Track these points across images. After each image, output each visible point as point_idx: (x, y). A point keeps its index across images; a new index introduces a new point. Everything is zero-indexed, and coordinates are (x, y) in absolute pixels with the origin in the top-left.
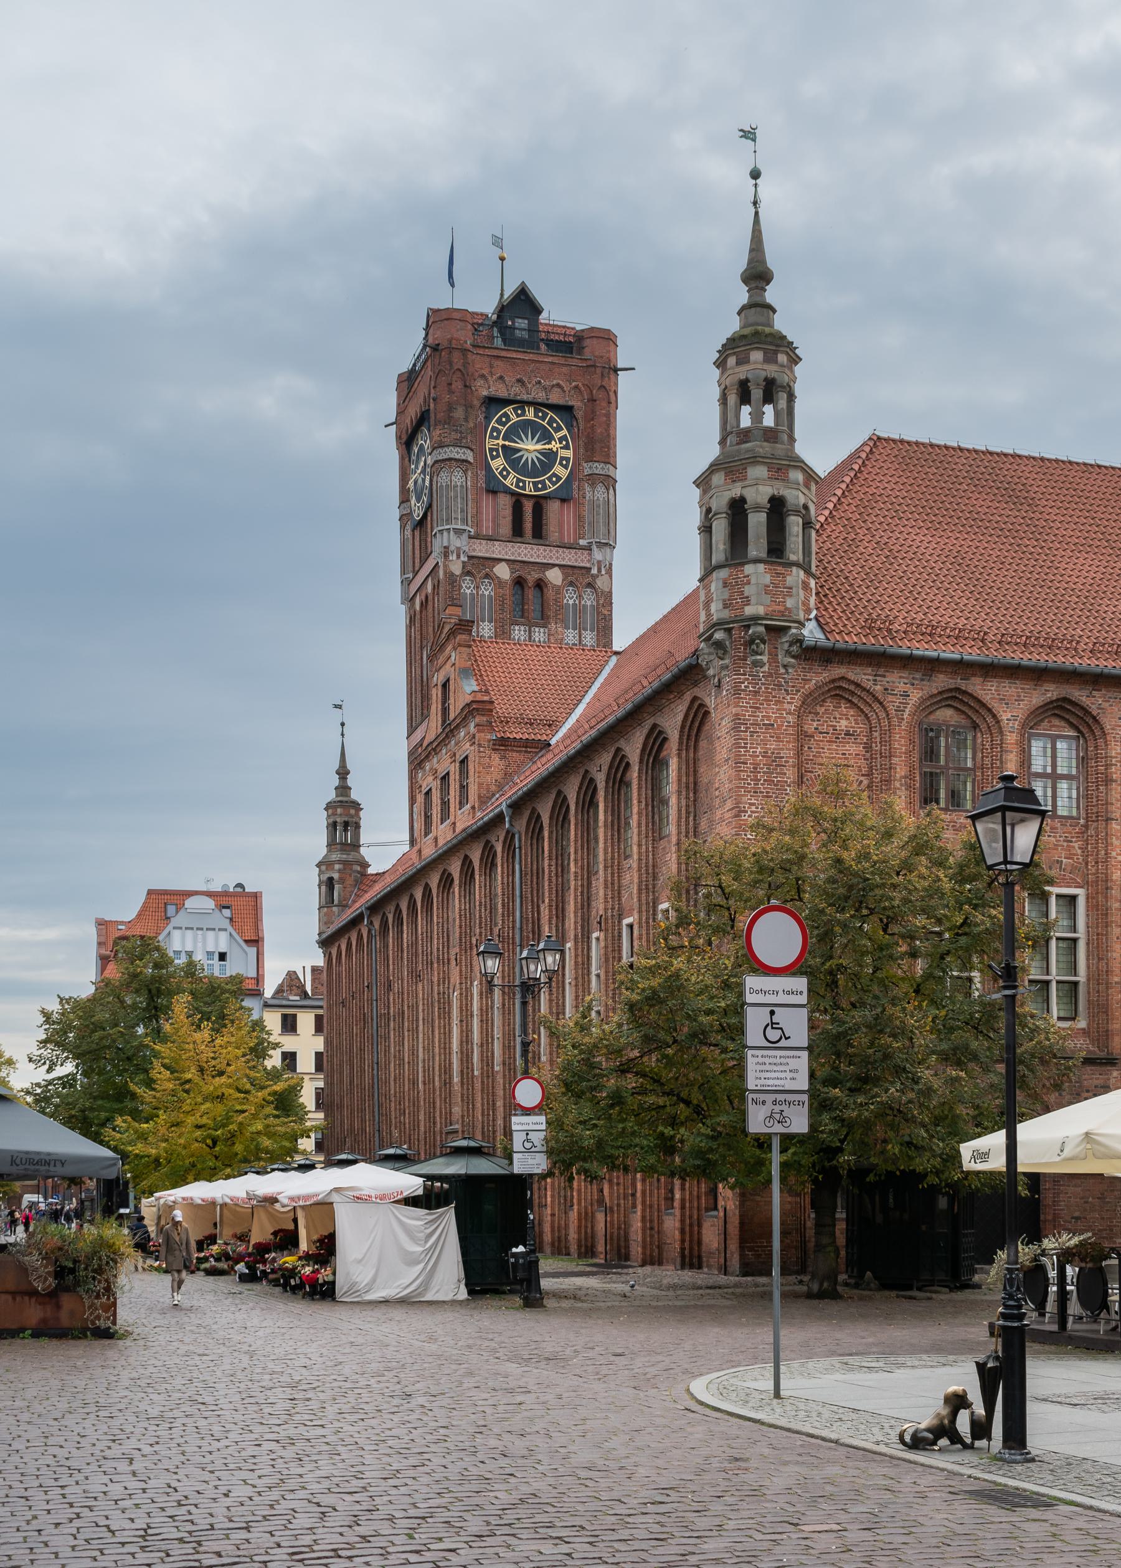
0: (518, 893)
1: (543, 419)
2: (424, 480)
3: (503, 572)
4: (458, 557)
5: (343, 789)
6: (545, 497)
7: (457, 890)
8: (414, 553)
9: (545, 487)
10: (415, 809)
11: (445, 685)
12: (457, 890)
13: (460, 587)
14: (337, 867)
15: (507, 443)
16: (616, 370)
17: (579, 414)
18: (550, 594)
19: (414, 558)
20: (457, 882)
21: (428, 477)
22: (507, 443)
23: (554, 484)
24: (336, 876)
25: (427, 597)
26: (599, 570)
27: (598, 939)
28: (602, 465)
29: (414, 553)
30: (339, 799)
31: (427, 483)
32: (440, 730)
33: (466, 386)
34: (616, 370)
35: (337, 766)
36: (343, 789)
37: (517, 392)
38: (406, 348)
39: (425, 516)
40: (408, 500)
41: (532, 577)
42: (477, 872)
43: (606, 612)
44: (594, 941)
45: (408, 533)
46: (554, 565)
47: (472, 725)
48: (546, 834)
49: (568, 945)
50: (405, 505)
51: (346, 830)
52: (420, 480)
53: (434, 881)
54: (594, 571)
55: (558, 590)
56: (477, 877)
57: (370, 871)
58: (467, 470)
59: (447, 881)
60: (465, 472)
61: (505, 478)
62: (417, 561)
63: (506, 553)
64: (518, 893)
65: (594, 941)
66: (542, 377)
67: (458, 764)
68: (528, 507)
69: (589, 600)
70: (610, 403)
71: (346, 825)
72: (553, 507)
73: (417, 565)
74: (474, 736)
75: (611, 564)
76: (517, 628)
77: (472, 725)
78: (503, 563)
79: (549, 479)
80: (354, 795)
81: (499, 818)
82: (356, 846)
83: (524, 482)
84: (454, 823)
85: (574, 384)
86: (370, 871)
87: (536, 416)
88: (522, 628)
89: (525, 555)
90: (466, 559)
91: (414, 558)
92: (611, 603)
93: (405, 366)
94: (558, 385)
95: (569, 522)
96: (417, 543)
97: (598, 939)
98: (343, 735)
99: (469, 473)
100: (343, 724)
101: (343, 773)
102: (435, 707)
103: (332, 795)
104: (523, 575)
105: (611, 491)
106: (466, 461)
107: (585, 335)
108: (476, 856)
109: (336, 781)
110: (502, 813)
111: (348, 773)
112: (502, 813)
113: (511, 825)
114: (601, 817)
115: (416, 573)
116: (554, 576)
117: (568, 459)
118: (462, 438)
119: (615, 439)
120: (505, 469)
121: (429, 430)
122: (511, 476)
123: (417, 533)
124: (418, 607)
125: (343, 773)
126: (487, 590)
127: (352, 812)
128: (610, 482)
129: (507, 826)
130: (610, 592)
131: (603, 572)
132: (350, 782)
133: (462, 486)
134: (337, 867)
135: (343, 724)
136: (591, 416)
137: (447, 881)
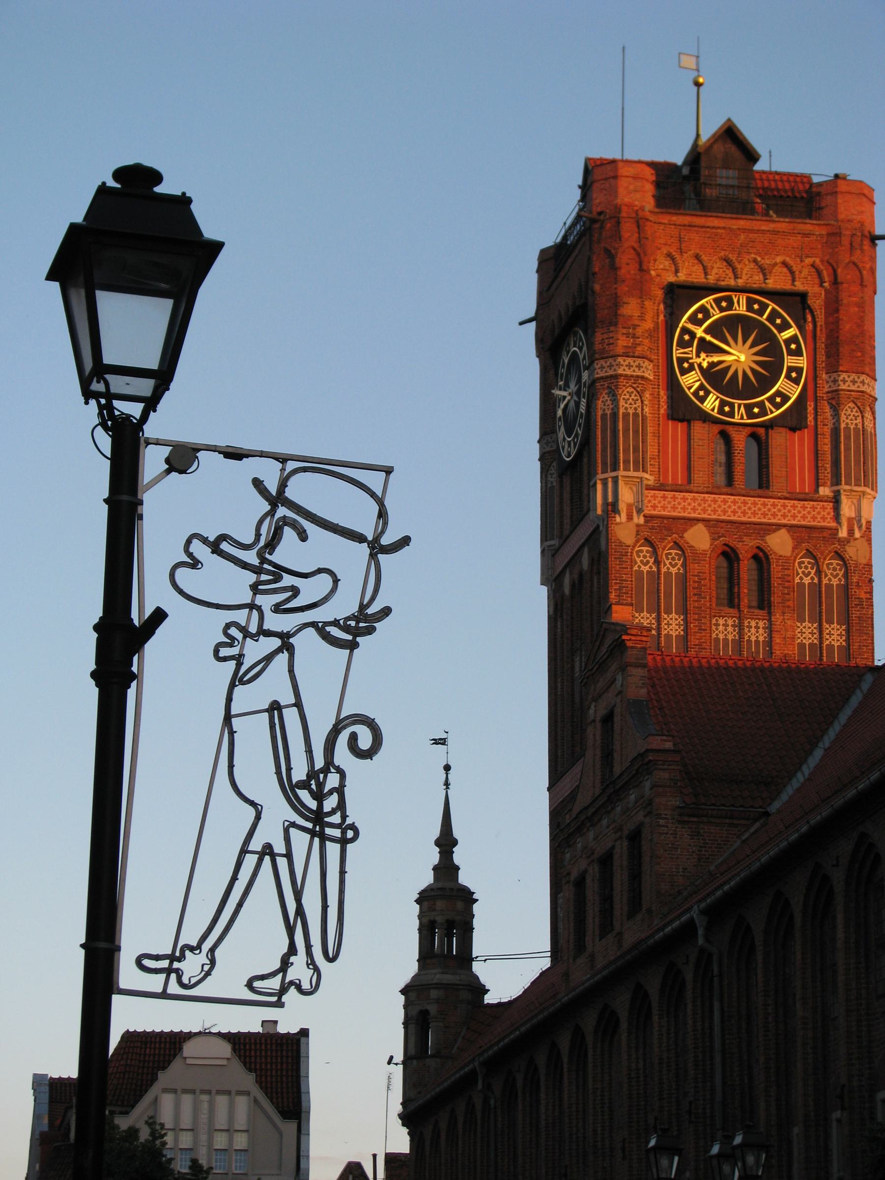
0: (717, 1045)
1: (761, 313)
2: (577, 404)
3: (699, 539)
4: (630, 518)
5: (446, 869)
6: (769, 426)
7: (624, 1036)
8: (561, 510)
9: (763, 412)
10: (560, 901)
11: (608, 719)
12: (624, 1036)
13: (633, 562)
14: (434, 994)
15: (708, 338)
16: (874, 239)
17: (817, 302)
18: (776, 570)
19: (561, 517)
20: (624, 1025)
21: (584, 402)
22: (708, 338)
23: (778, 406)
24: (433, 1009)
25: (581, 575)
26: (851, 532)
27: (839, 1121)
28: (853, 376)
29: (561, 510)
30: (440, 885)
31: (583, 409)
32: (598, 791)
33: (641, 269)
34: (874, 239)
35: (436, 832)
36: (446, 869)
37: (717, 273)
38: (553, 215)
39: (579, 455)
40: (554, 432)
41: (745, 547)
42: (655, 1011)
43: (863, 596)
44: (834, 1124)
45: (553, 479)
46: (779, 526)
47: (647, 784)
48: (759, 956)
49: (796, 1130)
50: (548, 438)
51: (450, 937)
52: (572, 404)
53: (589, 1021)
54: (843, 533)
55: (787, 563)
56: (655, 1018)
57: (489, 999)
58: (643, 391)
59: (608, 1024)
60: (640, 394)
61: (702, 400)
62: (567, 521)
63: (704, 510)
64: (717, 1045)
65: (834, 1124)
66: (758, 253)
67: (626, 843)
68: (740, 439)
69: (834, 578)
70: (862, 284)
71: (450, 926)
72: (778, 439)
73: (567, 527)
74: (650, 803)
75: (869, 523)
76: (721, 621)
77: (647, 784)
78: (700, 526)
79: (771, 399)
80: (464, 878)
81: (689, 928)
82: (466, 958)
83: (732, 406)
84: (620, 934)
85: (808, 261)
86: (489, 999)
87: (750, 308)
88: (730, 622)
89: (734, 512)
90: (641, 520)
91: (561, 517)
92: (871, 581)
93: (551, 236)
94: (785, 264)
95: (801, 458)
96: (567, 496)
97: (839, 1121)
98: (447, 784)
99: (647, 395)
100: (447, 768)
101: (446, 842)
102: (592, 754)
103: (427, 879)
104: (732, 543)
105: (868, 415)
106: (643, 378)
107: (822, 190)
108: (653, 984)
109: (434, 856)
110: (691, 921)
111: (455, 843)
112: (691, 921)
113: (707, 940)
114: (840, 934)
115: (564, 540)
116: (780, 544)
117: (799, 370)
118: (635, 345)
119: (872, 337)
120: (701, 387)
121: (586, 333)
122: (711, 398)
123: (567, 481)
124: (567, 590)
125: (446, 842)
126: (672, 566)
127: (460, 905)
128: (866, 403)
129: (701, 941)
130: (869, 565)
131: (857, 534)
132: (459, 856)
133: (635, 415)
134: (434, 994)
135: (447, 768)
136: (833, 305)
137: (608, 1024)
